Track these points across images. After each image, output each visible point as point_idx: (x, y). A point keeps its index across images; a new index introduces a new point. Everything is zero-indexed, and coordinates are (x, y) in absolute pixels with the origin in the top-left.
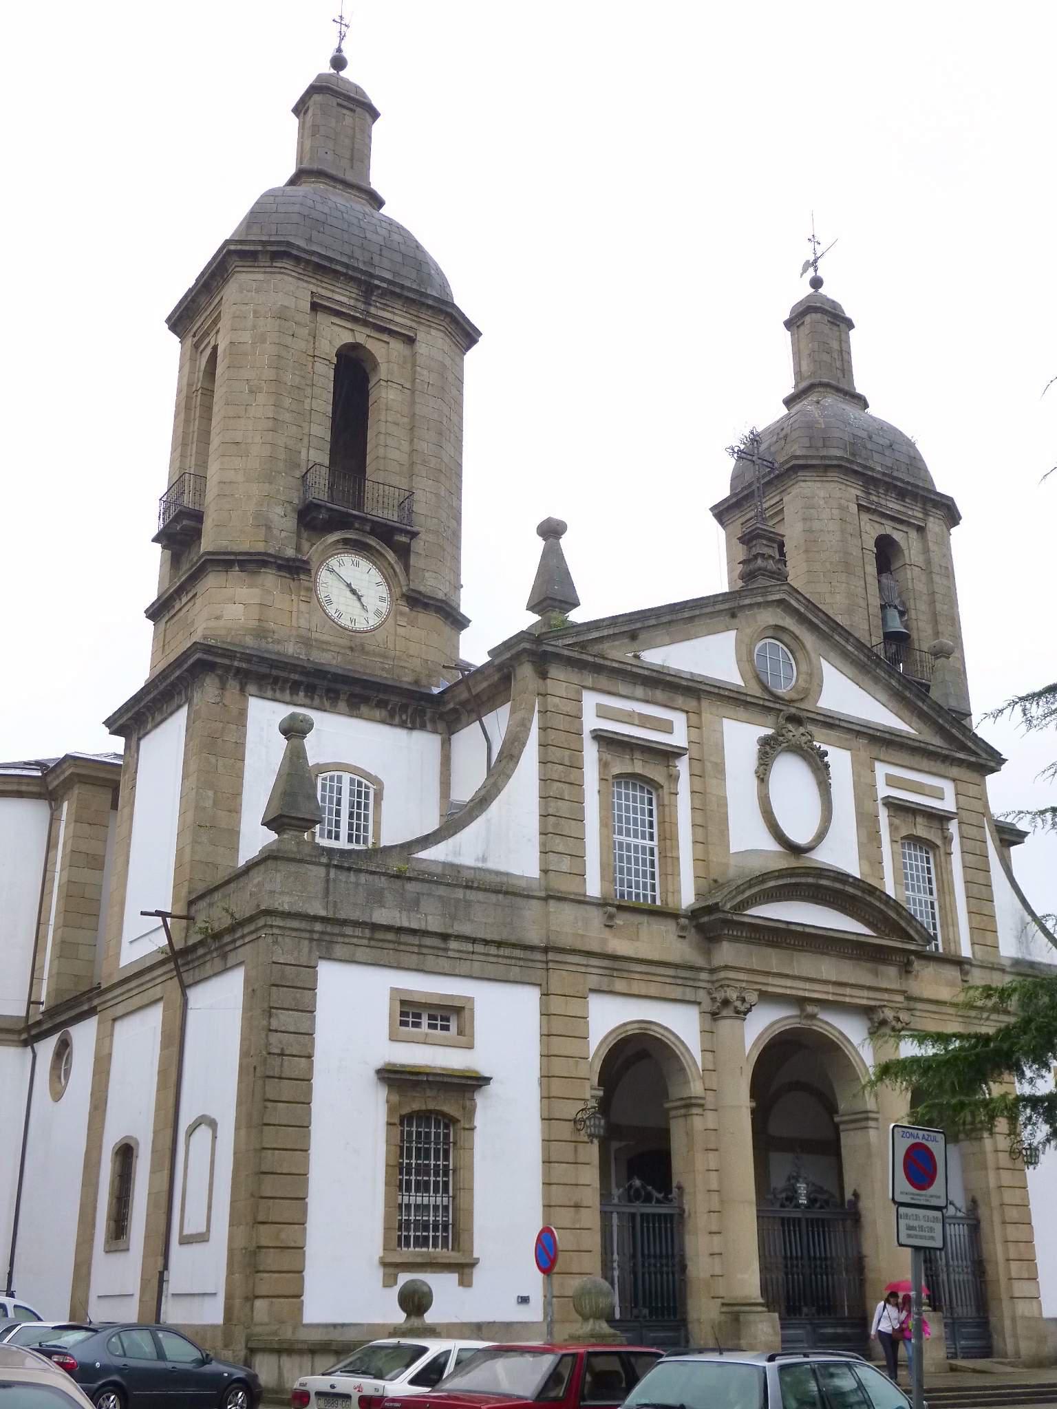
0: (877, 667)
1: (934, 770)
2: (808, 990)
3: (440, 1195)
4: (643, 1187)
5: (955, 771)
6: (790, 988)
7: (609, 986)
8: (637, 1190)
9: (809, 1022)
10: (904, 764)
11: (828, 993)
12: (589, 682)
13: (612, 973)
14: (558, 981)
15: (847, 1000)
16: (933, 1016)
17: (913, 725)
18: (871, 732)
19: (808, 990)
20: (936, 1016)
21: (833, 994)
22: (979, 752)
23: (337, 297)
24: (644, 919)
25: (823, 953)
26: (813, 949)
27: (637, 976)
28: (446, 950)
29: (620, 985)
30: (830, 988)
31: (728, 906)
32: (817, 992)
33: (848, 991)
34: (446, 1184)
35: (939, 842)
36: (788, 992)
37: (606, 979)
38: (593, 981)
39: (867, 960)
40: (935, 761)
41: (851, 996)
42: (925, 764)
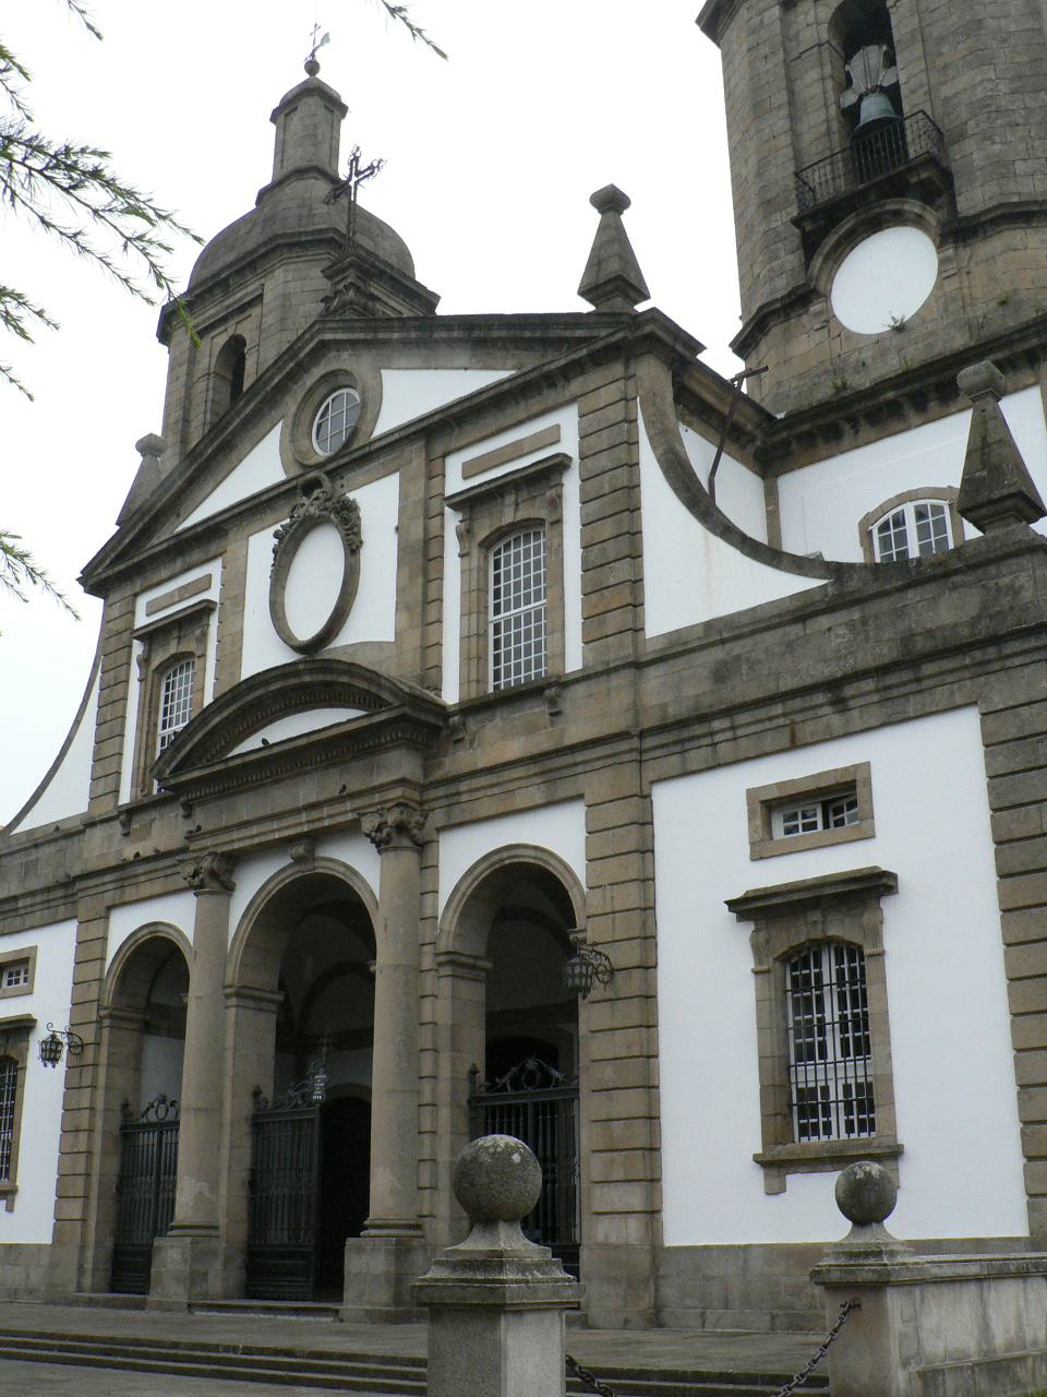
0: (432, 331)
1: (536, 408)
2: (278, 830)
3: (852, 1057)
4: (540, 1067)
5: (576, 386)
6: (257, 835)
7: (120, 898)
8: (532, 1073)
9: (310, 866)
10: (489, 431)
11: (301, 824)
12: (137, 587)
13: (121, 884)
14: (85, 906)
15: (326, 823)
16: (489, 792)
17: (508, 366)
18: (413, 429)
19: (278, 830)
20: (496, 790)
21: (308, 822)
22: (595, 333)
23: (207, 314)
24: (154, 814)
25: (299, 775)
26: (285, 775)
27: (143, 878)
28: (17, 909)
29: (130, 894)
30: (304, 817)
31: (168, 771)
32: (302, 824)
33: (326, 811)
34: (823, 1045)
35: (542, 514)
36: (256, 841)
37: (118, 892)
38: (108, 898)
39: (355, 758)
40: (540, 393)
41: (330, 816)
42: (521, 411)
